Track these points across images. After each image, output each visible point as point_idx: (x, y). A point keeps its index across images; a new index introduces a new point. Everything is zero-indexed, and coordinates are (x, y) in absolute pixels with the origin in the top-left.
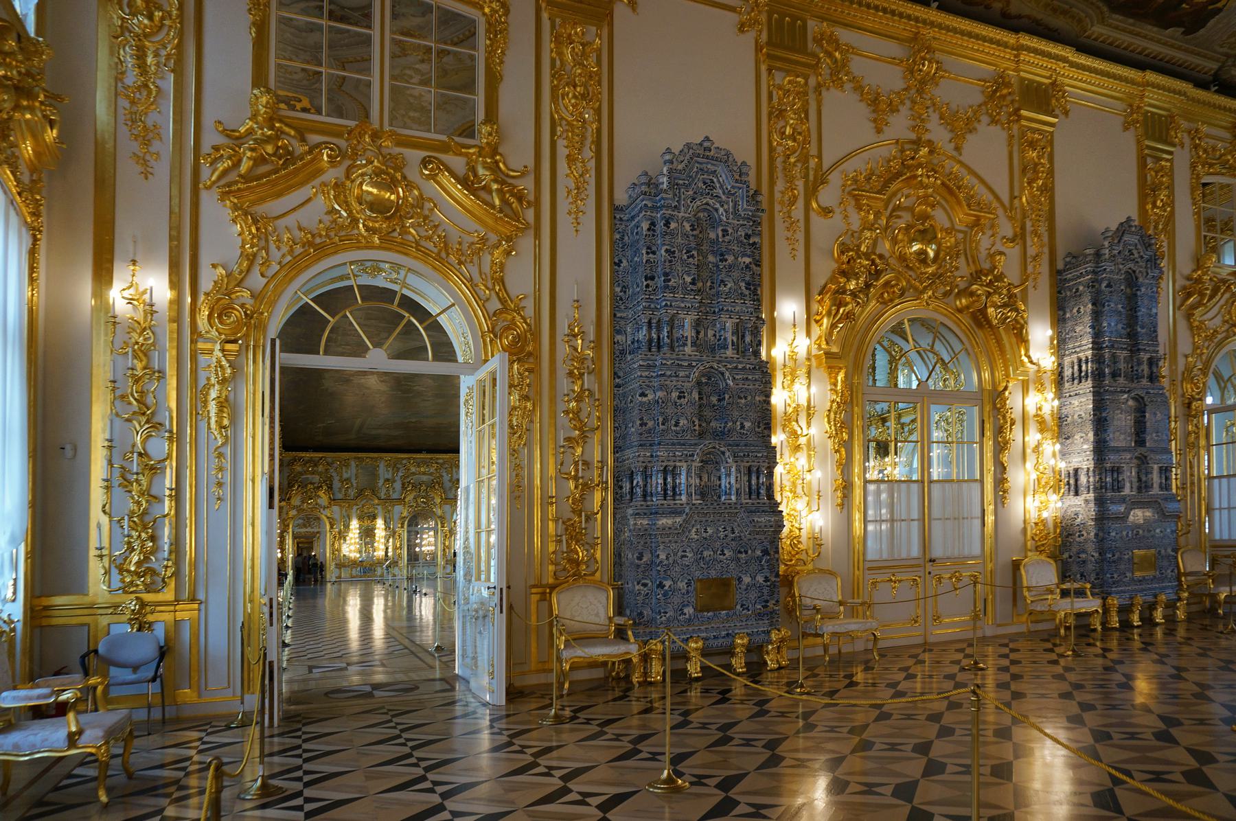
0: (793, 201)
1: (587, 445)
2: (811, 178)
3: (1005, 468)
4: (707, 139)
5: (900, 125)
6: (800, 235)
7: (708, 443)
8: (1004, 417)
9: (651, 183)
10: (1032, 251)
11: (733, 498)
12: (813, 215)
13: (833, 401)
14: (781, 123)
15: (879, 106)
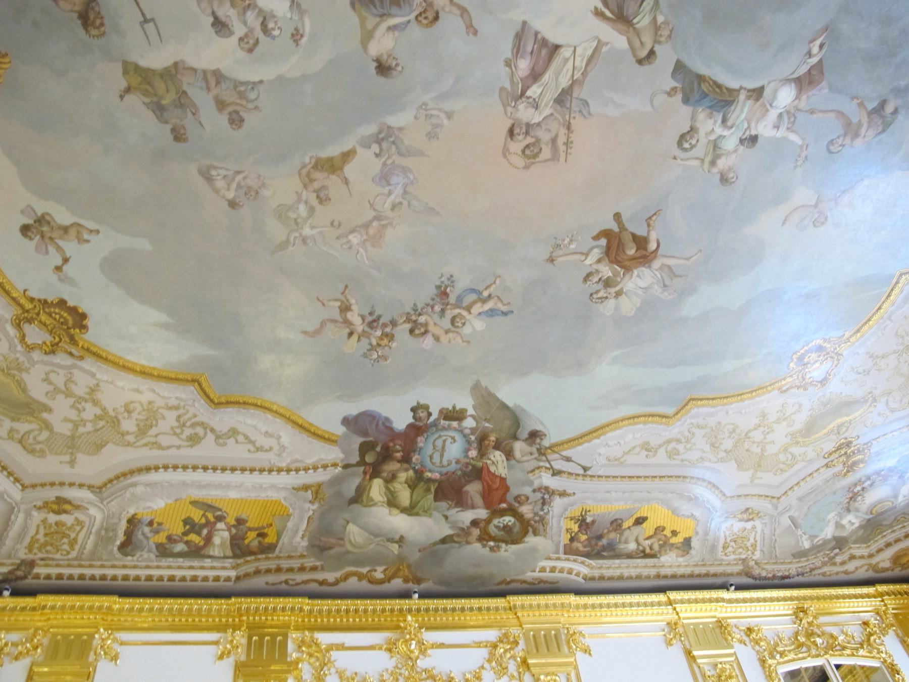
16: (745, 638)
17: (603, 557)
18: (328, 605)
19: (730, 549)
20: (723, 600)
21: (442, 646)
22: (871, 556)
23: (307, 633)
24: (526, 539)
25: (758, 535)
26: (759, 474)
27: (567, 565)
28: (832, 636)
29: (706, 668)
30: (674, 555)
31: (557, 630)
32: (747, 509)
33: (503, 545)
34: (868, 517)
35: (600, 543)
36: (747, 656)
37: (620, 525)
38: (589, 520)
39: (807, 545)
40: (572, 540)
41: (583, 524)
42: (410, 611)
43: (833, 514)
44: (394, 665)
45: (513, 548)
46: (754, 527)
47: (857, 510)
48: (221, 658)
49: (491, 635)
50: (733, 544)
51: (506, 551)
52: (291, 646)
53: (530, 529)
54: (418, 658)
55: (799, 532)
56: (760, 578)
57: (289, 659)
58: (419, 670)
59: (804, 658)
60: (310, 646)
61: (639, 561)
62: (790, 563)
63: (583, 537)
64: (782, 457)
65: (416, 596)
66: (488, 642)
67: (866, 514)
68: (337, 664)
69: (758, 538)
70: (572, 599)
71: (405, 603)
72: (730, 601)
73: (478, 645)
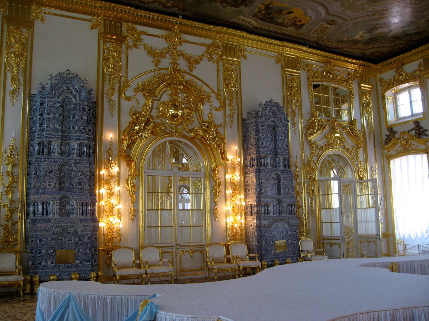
0: (113, 94)
1: (14, 194)
2: (122, 85)
3: (216, 203)
4: (68, 70)
5: (165, 62)
6: (116, 107)
7: (63, 192)
8: (216, 181)
9: (43, 88)
10: (228, 112)
11: (74, 215)
12: (122, 99)
13: (129, 175)
14: (109, 63)
15: (156, 55)
16: (305, 68)
17: (266, 22)
18: (142, 13)
19: (317, 32)
20: (303, 50)
21: (188, 42)
22: (365, 50)
23: (130, 23)
24: (240, 7)
25: (331, 30)
26: (346, 10)
27: (249, 20)
28: (336, 76)
29: (288, 76)
30: (294, 28)
31: (236, 46)
32: (333, 21)
33: (229, 6)
34: (374, 37)
35: (269, 16)
36: (304, 75)
37: (281, 12)
38: (271, 6)
39: (345, 39)
40: (258, 12)
41: (267, 7)
42: (177, 23)
43: (362, 32)
44: (168, 46)
45: (233, 8)
46: (331, 28)
47: (372, 33)
48: (92, 28)
49: (208, 41)
50: (319, 31)
51: (229, 9)
52: (124, 29)
53: (245, 3)
54: (178, 45)
55: (346, 34)
56: (320, 45)
57: (123, 35)
58: (177, 51)
59: (323, 81)
60: (132, 31)
61: (279, 26)
62: (335, 43)
63: (264, 12)
64: (359, 7)
65: (181, 17)
66: (207, 44)
67: (374, 35)
68: (143, 41)
69: (329, 32)
70: (244, 34)
71: (174, 19)
72: (305, 51)
73: (203, 45)
